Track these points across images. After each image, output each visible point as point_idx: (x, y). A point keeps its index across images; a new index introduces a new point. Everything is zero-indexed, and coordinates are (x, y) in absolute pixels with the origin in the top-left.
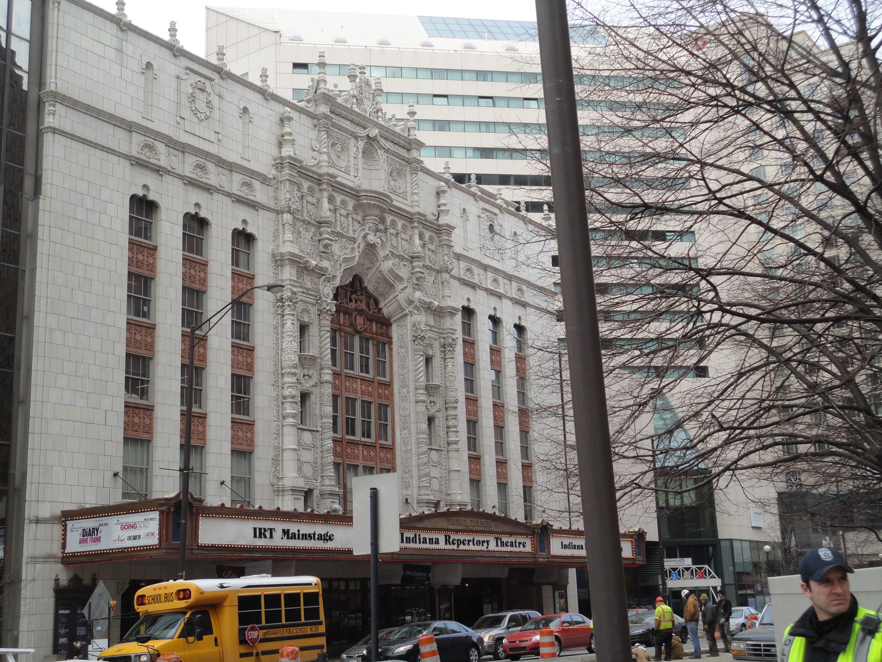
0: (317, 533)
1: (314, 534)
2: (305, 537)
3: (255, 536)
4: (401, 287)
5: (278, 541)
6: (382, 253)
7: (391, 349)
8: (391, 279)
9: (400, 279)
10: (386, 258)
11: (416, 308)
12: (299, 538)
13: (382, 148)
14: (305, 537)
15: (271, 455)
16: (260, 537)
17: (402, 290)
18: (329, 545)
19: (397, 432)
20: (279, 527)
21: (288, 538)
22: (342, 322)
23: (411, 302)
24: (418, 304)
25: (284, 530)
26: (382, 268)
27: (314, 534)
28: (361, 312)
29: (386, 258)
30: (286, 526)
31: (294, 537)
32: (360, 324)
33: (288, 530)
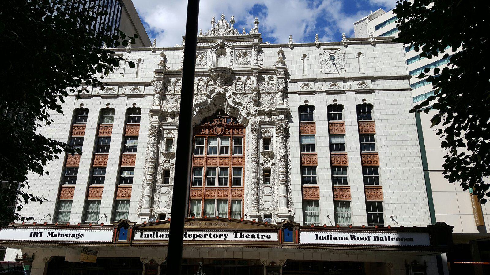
0: (72, 234)
1: (70, 234)
2: (63, 236)
3: (31, 236)
4: (242, 107)
5: (45, 237)
6: (228, 94)
7: (244, 139)
8: (235, 106)
9: (241, 104)
10: (230, 97)
11: (253, 115)
12: (59, 236)
13: (229, 47)
14: (63, 236)
15: (139, 199)
16: (34, 236)
17: (243, 109)
18: (80, 239)
19: (245, 180)
20: (46, 232)
21: (52, 236)
22: (207, 133)
23: (249, 114)
24: (254, 113)
25: (49, 233)
26: (229, 102)
27: (70, 234)
28: (219, 126)
29: (230, 97)
30: (51, 231)
31: (56, 236)
32: (219, 131)
33: (52, 233)
